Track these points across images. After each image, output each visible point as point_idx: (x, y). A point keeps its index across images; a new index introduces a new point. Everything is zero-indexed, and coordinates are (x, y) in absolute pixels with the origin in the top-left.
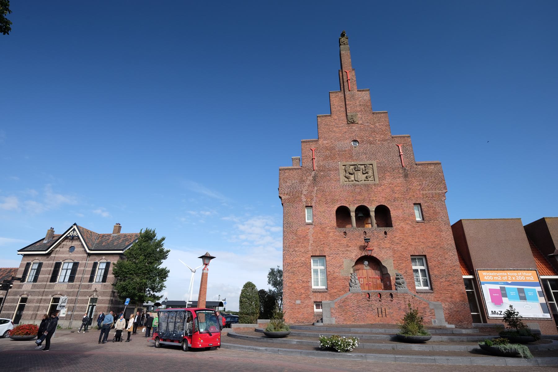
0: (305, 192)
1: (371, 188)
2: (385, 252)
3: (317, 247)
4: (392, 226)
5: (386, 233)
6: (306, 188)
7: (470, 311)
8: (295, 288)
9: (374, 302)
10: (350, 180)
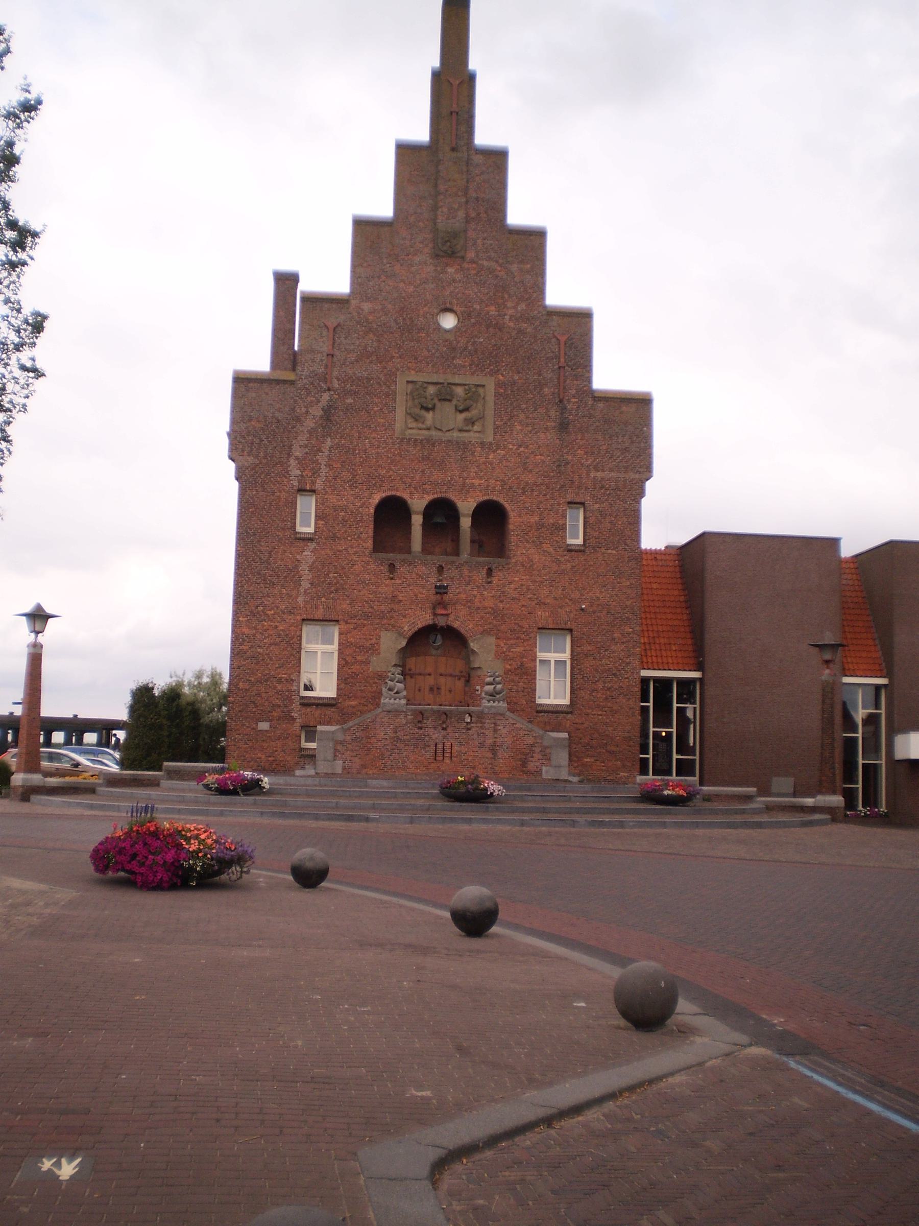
0: (298, 452)
2: (482, 618)
3: (319, 598)
5: (490, 572)
6: (303, 439)
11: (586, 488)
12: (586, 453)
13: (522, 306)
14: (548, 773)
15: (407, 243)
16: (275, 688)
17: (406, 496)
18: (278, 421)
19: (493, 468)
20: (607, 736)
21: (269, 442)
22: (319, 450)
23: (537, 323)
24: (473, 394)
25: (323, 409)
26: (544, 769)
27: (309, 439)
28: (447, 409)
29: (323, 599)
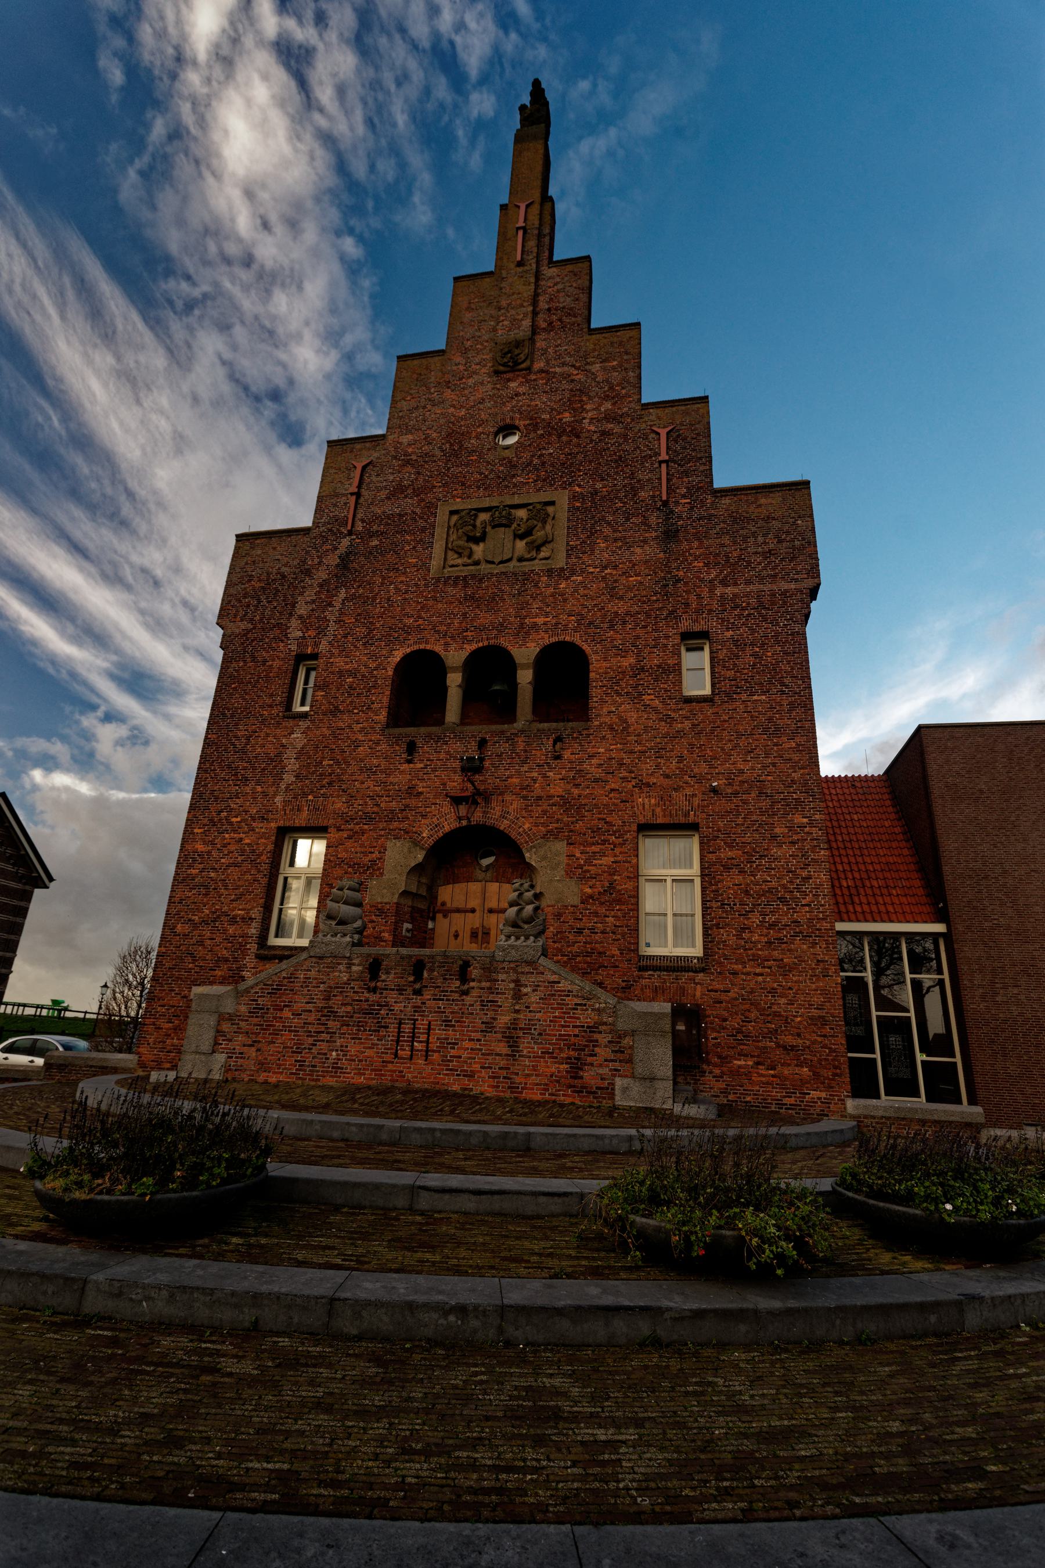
0: (302, 610)
1: (536, 586)
2: (545, 812)
6: (310, 594)
7: (843, 1049)
8: (200, 943)
9: (392, 997)
11: (710, 611)
12: (706, 565)
13: (608, 405)
14: (628, 1094)
15: (461, 367)
16: (225, 930)
17: (438, 648)
18: (284, 577)
19: (565, 600)
20: (776, 1014)
21: (269, 602)
22: (330, 605)
24: (541, 513)
25: (340, 557)
26: (619, 1082)
27: (318, 593)
28: (503, 535)
29: (310, 797)
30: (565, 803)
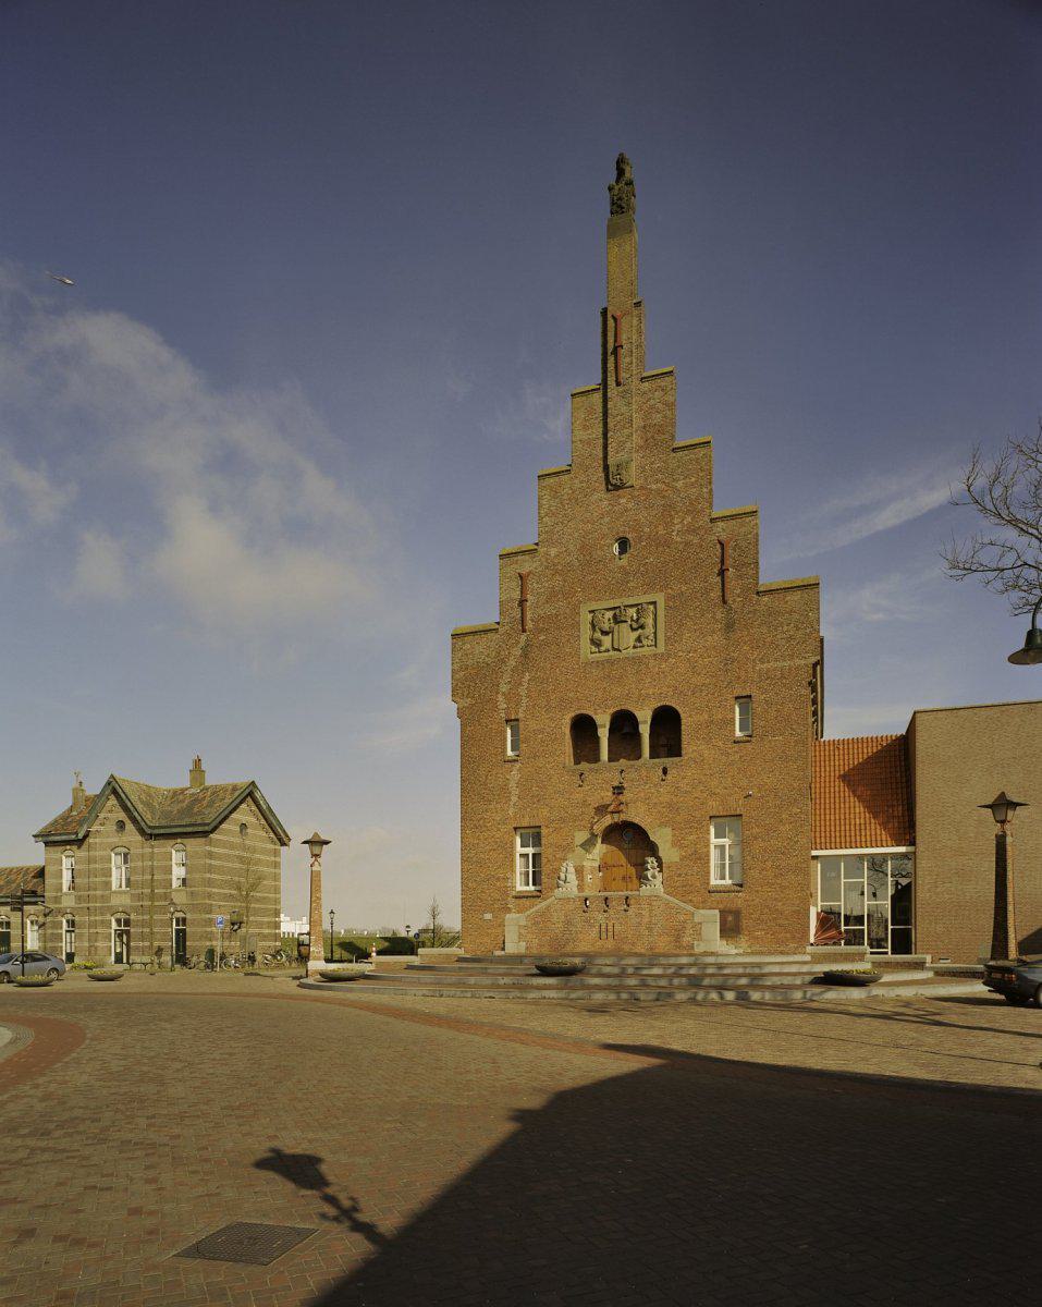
0: (504, 688)
4: (679, 754)
5: (665, 771)
10: (603, 649)
17: (590, 713)
22: (520, 684)
23: (702, 533)
30: (670, 805)
